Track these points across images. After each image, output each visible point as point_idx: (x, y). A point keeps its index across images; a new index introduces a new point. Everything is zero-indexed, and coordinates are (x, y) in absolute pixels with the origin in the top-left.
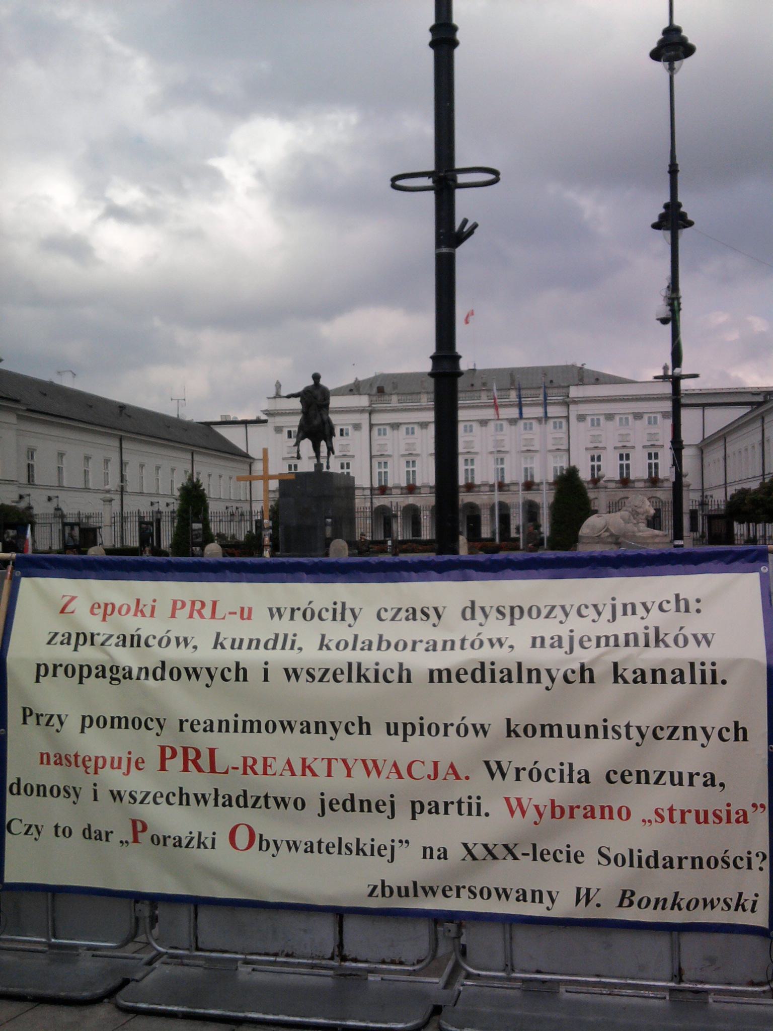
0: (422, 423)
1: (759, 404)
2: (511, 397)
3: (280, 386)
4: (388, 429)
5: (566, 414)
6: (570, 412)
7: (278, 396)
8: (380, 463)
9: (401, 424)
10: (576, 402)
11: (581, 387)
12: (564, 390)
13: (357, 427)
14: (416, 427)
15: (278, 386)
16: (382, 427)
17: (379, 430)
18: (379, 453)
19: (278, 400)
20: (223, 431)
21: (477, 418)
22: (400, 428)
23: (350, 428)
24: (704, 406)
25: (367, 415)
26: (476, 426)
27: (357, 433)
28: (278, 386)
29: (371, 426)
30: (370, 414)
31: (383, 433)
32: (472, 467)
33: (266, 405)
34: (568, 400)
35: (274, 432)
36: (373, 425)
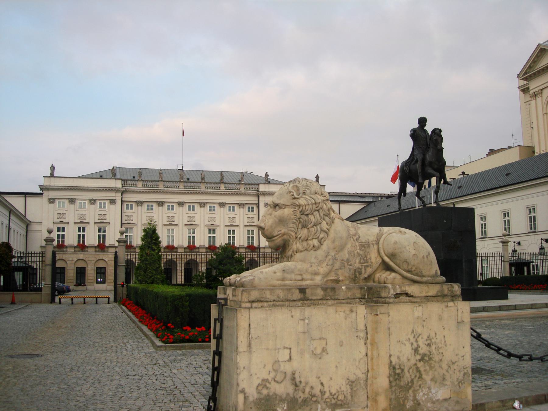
0: (160, 202)
1: (369, 203)
2: (221, 188)
3: (54, 168)
4: (134, 205)
5: (257, 203)
6: (260, 201)
7: (52, 175)
10: (265, 194)
11: (267, 185)
12: (256, 186)
13: (113, 202)
15: (53, 168)
16: (129, 204)
17: (127, 205)
18: (126, 222)
19: (52, 179)
20: (12, 200)
22: (143, 205)
23: (107, 202)
24: (339, 202)
26: (197, 207)
27: (113, 207)
28: (53, 168)
29: (122, 202)
33: (42, 182)
34: (259, 193)
35: (48, 203)
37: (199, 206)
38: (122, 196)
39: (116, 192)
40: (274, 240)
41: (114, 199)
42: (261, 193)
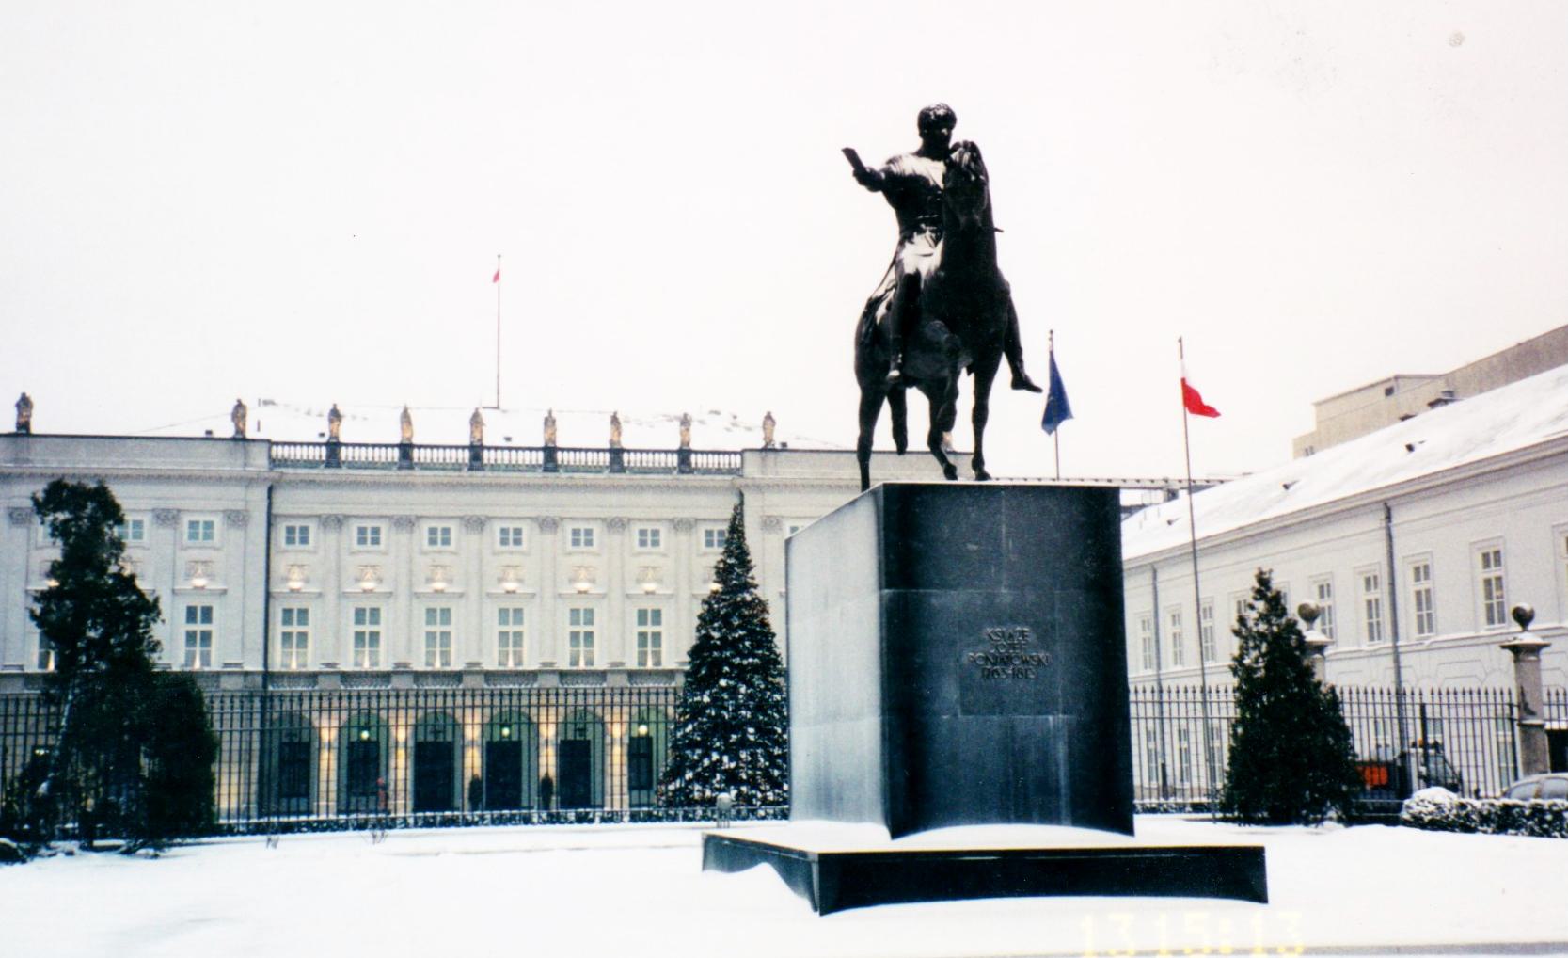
8: (288, 612)
9: (347, 517)
13: (237, 518)
14: (384, 527)
15: (24, 404)
19: (23, 442)
21: (534, 514)
25: (259, 494)
27: (236, 535)
28: (24, 404)
29: (271, 520)
30: (270, 490)
31: (298, 536)
32: (517, 628)
34: (739, 481)
36: (276, 516)
37: (536, 526)
38: (270, 497)
39: (247, 487)
40: (269, 770)
41: (240, 506)
42: (750, 482)
